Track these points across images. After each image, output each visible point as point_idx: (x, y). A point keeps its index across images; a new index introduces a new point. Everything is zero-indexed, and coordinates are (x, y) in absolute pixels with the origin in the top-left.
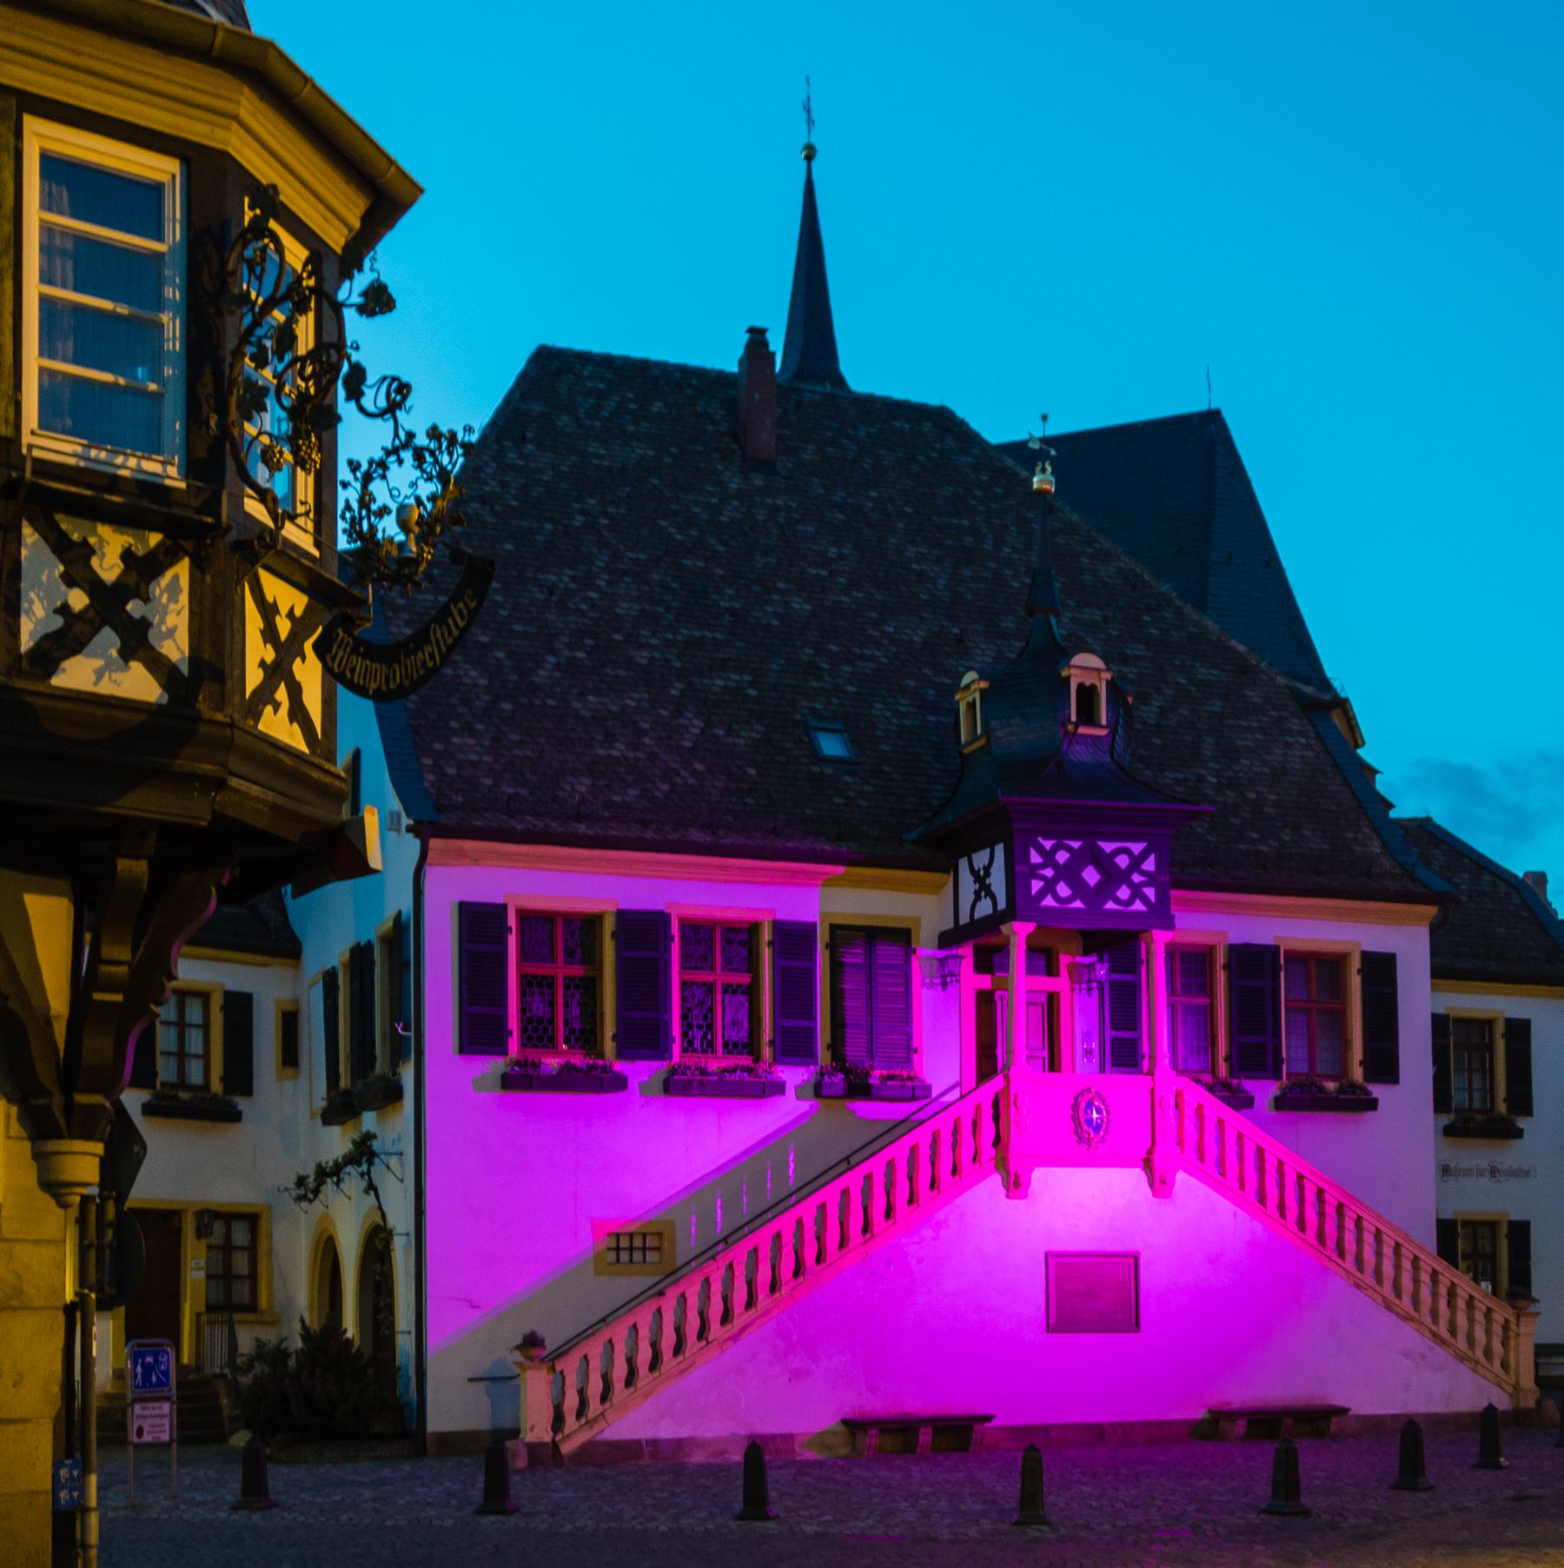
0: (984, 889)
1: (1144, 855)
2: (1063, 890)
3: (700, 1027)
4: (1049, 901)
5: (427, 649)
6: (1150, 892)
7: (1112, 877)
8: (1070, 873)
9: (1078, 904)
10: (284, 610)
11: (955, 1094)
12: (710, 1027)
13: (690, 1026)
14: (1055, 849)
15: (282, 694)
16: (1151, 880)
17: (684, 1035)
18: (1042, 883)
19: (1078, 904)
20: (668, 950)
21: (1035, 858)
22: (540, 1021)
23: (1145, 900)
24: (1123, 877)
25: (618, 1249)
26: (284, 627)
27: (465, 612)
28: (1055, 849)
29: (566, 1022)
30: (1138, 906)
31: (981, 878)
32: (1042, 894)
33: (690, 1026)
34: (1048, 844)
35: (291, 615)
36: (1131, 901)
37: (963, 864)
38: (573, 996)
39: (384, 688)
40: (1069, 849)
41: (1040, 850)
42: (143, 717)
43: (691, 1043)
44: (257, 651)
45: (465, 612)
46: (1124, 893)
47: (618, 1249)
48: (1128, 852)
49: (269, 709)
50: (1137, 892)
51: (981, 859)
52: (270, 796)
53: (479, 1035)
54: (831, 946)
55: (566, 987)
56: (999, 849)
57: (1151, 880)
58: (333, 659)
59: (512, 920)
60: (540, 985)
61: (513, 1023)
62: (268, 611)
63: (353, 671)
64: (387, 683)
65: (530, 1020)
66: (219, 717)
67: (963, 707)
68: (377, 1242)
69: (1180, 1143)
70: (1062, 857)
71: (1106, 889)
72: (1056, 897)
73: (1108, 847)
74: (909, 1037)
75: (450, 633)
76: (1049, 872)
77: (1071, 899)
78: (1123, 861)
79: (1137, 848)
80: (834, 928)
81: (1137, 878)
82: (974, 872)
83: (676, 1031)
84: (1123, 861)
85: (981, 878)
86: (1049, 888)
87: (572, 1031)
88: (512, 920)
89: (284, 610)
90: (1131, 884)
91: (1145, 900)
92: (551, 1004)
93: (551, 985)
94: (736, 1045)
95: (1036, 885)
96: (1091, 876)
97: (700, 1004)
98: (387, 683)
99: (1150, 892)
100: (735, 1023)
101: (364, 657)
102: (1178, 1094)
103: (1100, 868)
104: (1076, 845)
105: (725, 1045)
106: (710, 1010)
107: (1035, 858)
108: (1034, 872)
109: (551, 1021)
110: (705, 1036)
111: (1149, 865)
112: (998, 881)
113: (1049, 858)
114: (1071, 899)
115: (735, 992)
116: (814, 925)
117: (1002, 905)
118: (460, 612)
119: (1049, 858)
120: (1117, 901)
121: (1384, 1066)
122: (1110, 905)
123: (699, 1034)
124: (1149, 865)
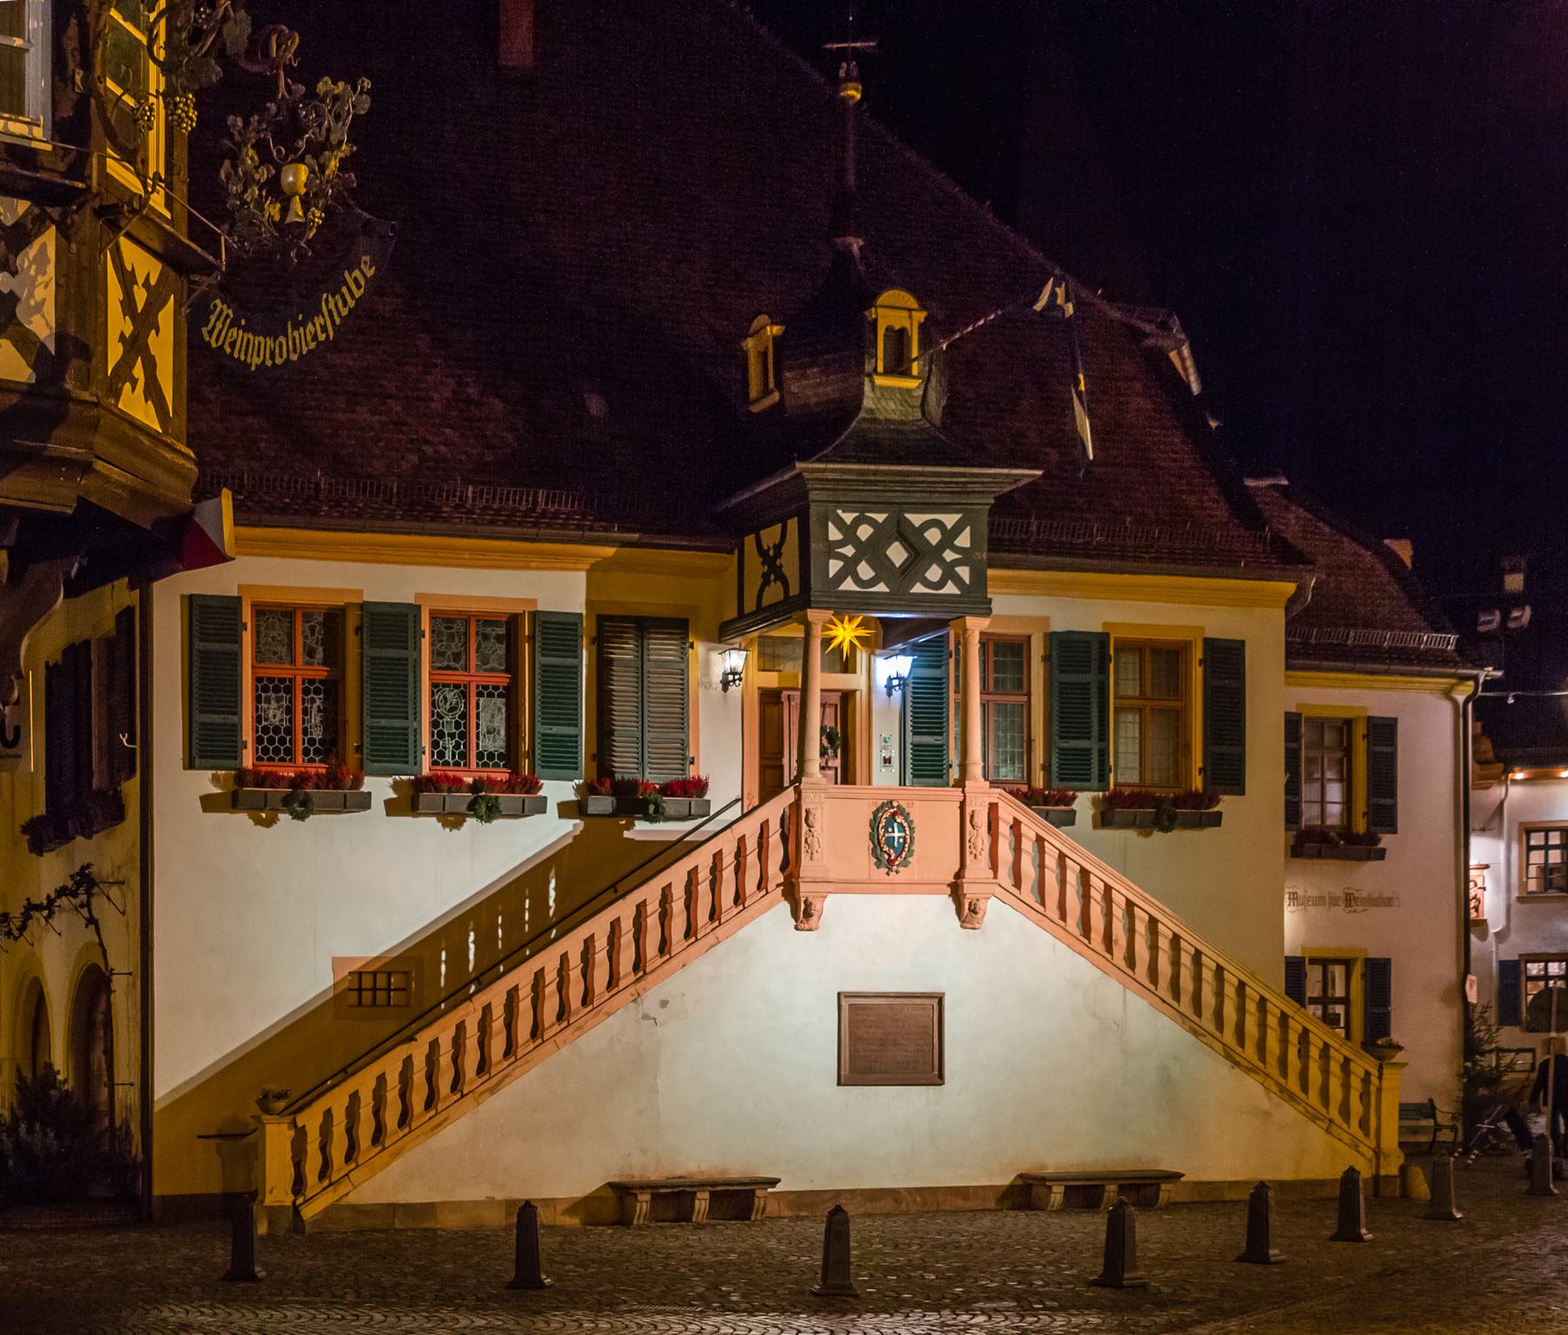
0: (773, 571)
1: (958, 529)
2: (865, 571)
3: (452, 736)
4: (848, 585)
5: (319, 321)
6: (964, 572)
7: (921, 554)
8: (873, 551)
9: (882, 588)
10: (141, 279)
11: (735, 812)
12: (463, 736)
13: (441, 735)
14: (857, 523)
15: (138, 371)
17: (435, 745)
18: (841, 564)
19: (882, 588)
20: (417, 648)
21: (834, 534)
22: (277, 730)
23: (958, 581)
24: (935, 554)
25: (360, 990)
26: (141, 296)
27: (362, 282)
28: (857, 523)
29: (305, 732)
30: (950, 589)
31: (770, 559)
32: (841, 577)
33: (441, 735)
34: (848, 518)
35: (146, 284)
36: (941, 584)
37: (750, 541)
38: (313, 701)
39: (269, 363)
40: (872, 522)
42: (15, 399)
43: (441, 755)
44: (118, 324)
45: (362, 282)
46: (934, 573)
47: (360, 990)
48: (939, 524)
49: (128, 385)
50: (949, 573)
51: (770, 536)
52: (128, 479)
55: (306, 691)
56: (793, 524)
57: (966, 556)
58: (210, 333)
59: (247, 616)
60: (276, 690)
61: (248, 735)
62: (127, 279)
63: (233, 345)
64: (272, 356)
65: (265, 730)
66: (86, 396)
67: (753, 360)
68: (93, 985)
69: (994, 866)
70: (864, 532)
71: (912, 570)
72: (858, 581)
73: (917, 519)
74: (684, 745)
75: (345, 303)
76: (849, 551)
78: (933, 536)
82: (762, 552)
83: (426, 742)
84: (933, 536)
85: (770, 559)
86: (849, 568)
87: (312, 742)
89: (141, 279)
92: (289, 711)
93: (289, 690)
94: (491, 756)
95: (835, 566)
96: (897, 554)
97: (452, 709)
98: (272, 356)
101: (246, 329)
102: (993, 807)
104: (880, 518)
105: (480, 756)
106: (463, 716)
107: (834, 534)
108: (831, 550)
109: (289, 731)
110: (457, 746)
112: (789, 562)
113: (849, 532)
115: (491, 695)
117: (794, 589)
118: (356, 280)
119: (849, 532)
120: (928, 584)
121: (1228, 772)
123: (450, 744)
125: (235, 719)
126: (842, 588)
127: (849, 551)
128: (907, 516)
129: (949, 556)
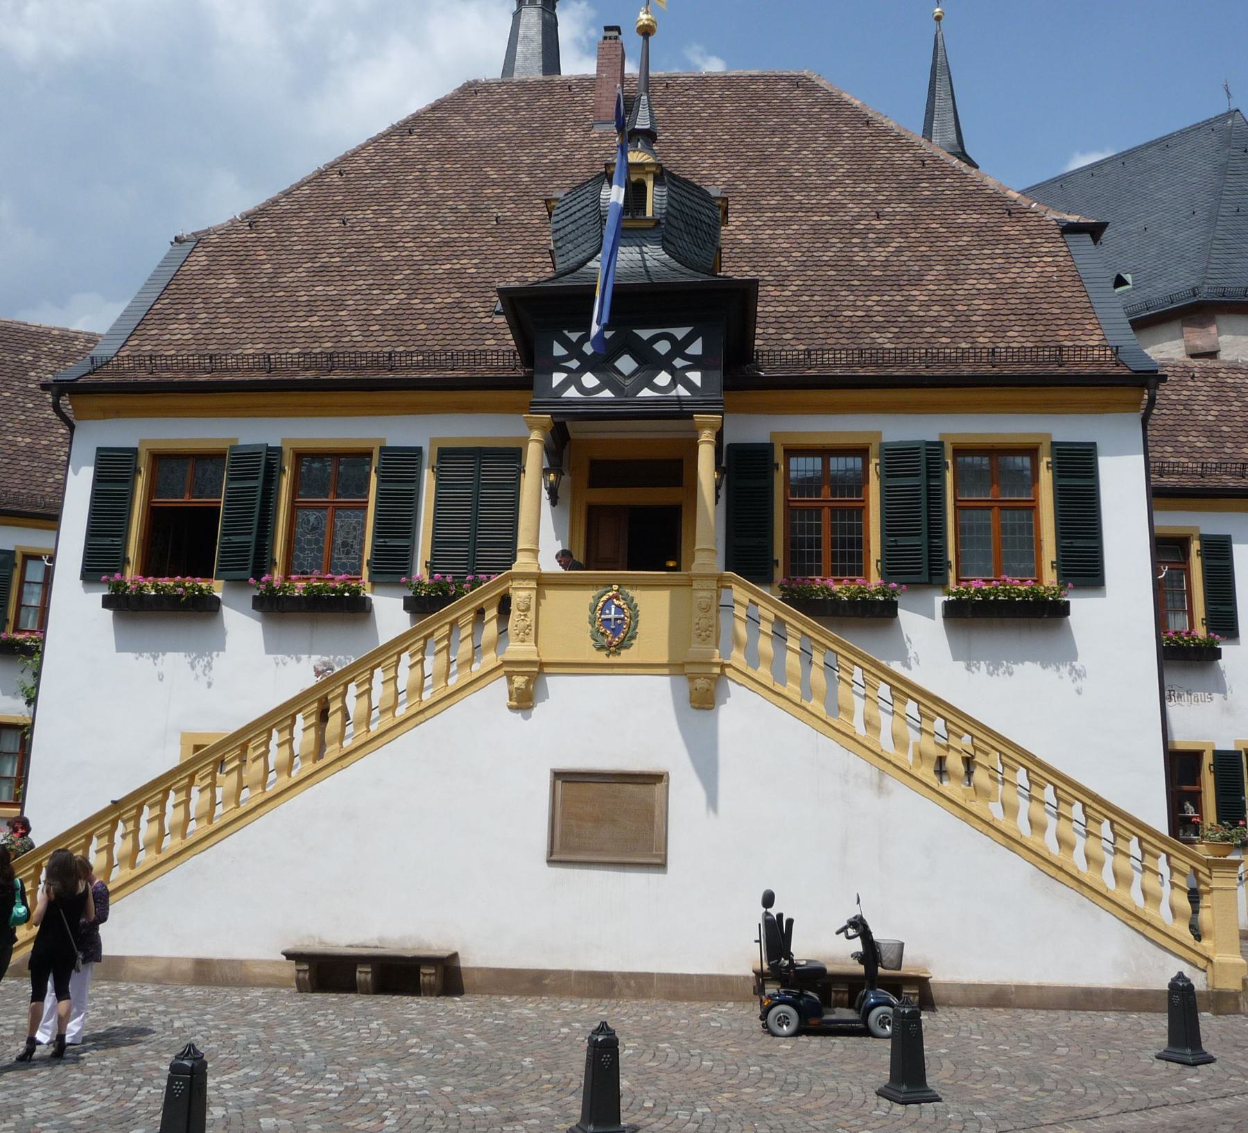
1: (689, 340)
2: (589, 380)
3: (312, 550)
4: (572, 393)
16: (696, 363)
18: (564, 375)
21: (559, 350)
23: (689, 385)
24: (664, 363)
30: (682, 391)
32: (564, 385)
41: (566, 343)
46: (663, 379)
53: (97, 565)
59: (143, 464)
72: (581, 388)
73: (645, 334)
76: (574, 364)
77: (597, 389)
78: (663, 347)
79: (680, 333)
84: (663, 347)
88: (143, 464)
90: (672, 370)
96: (626, 364)
100: (345, 544)
107: (559, 350)
111: (696, 348)
114: (597, 389)
119: (574, 350)
120: (654, 388)
122: (646, 393)
124: (696, 348)
125: (118, 541)
126: (565, 395)
129: (679, 363)
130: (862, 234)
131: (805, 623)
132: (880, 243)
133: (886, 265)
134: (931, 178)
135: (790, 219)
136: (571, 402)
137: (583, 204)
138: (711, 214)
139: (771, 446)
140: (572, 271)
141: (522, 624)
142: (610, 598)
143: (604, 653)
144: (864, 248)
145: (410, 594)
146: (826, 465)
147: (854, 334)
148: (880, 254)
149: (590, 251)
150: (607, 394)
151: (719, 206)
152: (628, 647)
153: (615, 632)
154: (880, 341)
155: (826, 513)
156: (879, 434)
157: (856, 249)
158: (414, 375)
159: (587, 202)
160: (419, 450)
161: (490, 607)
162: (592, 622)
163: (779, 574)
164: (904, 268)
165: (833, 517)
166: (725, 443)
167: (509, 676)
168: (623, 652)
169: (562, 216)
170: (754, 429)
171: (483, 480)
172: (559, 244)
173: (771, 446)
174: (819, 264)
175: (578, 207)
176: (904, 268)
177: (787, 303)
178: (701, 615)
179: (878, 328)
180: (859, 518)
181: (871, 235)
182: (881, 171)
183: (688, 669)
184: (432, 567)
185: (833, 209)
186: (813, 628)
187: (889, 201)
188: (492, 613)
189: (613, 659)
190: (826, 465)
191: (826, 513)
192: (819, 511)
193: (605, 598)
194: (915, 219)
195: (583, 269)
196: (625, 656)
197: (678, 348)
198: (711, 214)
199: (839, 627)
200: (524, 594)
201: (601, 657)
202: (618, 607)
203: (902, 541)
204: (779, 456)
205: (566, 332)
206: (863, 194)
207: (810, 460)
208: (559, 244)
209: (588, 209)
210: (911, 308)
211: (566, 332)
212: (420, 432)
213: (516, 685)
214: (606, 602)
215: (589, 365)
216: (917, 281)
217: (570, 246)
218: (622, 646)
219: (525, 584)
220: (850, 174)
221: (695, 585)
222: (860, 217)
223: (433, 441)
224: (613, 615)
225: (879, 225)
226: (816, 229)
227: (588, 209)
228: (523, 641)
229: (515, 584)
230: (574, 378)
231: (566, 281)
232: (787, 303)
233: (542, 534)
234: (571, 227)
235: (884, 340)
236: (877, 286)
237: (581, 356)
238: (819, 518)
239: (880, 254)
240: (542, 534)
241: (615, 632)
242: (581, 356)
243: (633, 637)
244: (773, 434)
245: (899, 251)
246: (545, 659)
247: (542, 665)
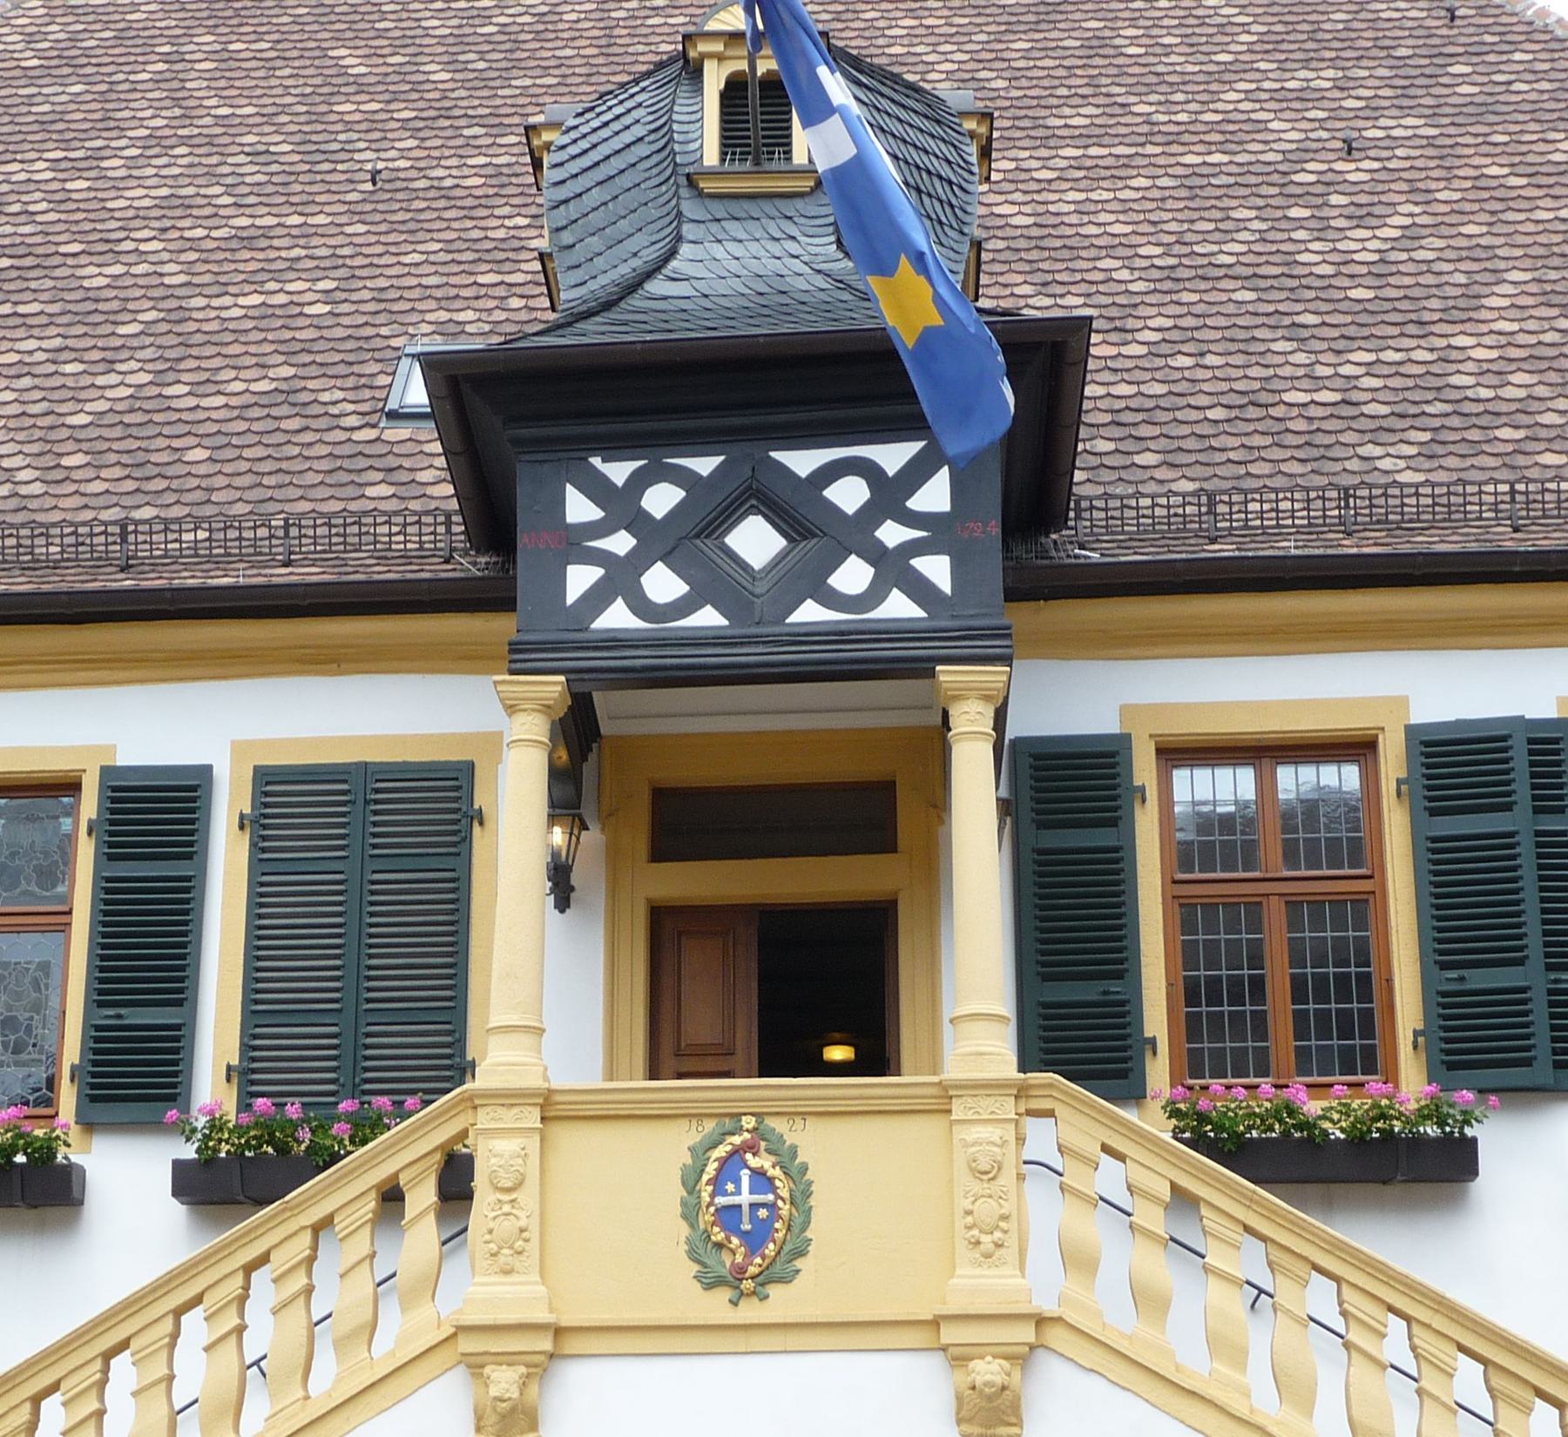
2: (662, 584)
4: (617, 617)
6: (937, 569)
14: (639, 483)
18: (599, 572)
21: (579, 508)
23: (920, 589)
24: (854, 534)
28: (639, 483)
30: (898, 606)
32: (597, 598)
34: (619, 472)
36: (874, 595)
41: (598, 489)
46: (853, 576)
54: (257, 824)
70: (661, 500)
72: (641, 605)
73: (802, 462)
77: (684, 607)
78: (849, 495)
80: (266, 779)
81: (892, 534)
84: (849, 495)
86: (621, 579)
90: (877, 555)
91: (920, 589)
96: (756, 541)
99: (937, 569)
103: (728, 516)
104: (705, 466)
107: (579, 508)
111: (935, 496)
114: (684, 607)
116: (205, 772)
119: (621, 507)
122: (810, 613)
124: (935, 496)
127: (621, 543)
128: (773, 454)
129: (892, 534)
130: (1317, 196)
131: (1250, 1202)
132: (1363, 217)
133: (1381, 271)
134: (1474, 53)
135: (1126, 163)
136: (616, 641)
137: (627, 137)
138: (952, 155)
139: (1124, 740)
140: (608, 305)
141: (507, 1227)
142: (737, 1152)
143: (724, 1294)
144: (1322, 229)
145: (189, 1152)
146: (1266, 786)
147: (1316, 449)
148: (1364, 245)
149: (651, 254)
150: (708, 618)
151: (972, 135)
152: (785, 1279)
153: (754, 1241)
154: (1386, 464)
155: (1275, 914)
156: (1402, 702)
157: (1300, 235)
158: (190, 580)
159: (639, 131)
160: (205, 772)
161: (417, 1181)
162: (690, 1213)
163: (1158, 1073)
164: (1429, 279)
165: (1294, 924)
166: (1010, 735)
167: (475, 1366)
168: (774, 1291)
169: (574, 167)
170: (1077, 697)
171: (379, 850)
172: (567, 237)
173: (1124, 740)
174: (1209, 275)
175: (616, 144)
176: (1429, 279)
177: (1138, 375)
178: (977, 1187)
179: (1379, 432)
180: (1361, 923)
181: (1335, 199)
182: (1347, 37)
183: (949, 1334)
184: (245, 1077)
185: (1232, 134)
186: (1271, 1215)
187: (1372, 112)
188: (422, 1197)
189: (750, 1312)
190: (1266, 786)
191: (1275, 914)
192: (1255, 908)
193: (721, 1151)
194: (1445, 156)
195: (635, 301)
196: (781, 1303)
197: (890, 496)
198: (952, 155)
199: (1327, 1206)
200: (506, 1146)
201: (716, 1306)
202: (758, 1173)
203: (1479, 979)
204: (1144, 769)
205: (596, 461)
206: (1304, 96)
207: (1224, 774)
208: (567, 237)
209: (642, 150)
210: (1456, 380)
211: (596, 461)
212: (218, 726)
213: (494, 1391)
214: (724, 1162)
215: (660, 540)
216: (1465, 309)
217: (595, 243)
218: (766, 1279)
219: (508, 1117)
220: (1269, 45)
221: (959, 1110)
222: (1307, 151)
223: (239, 749)
224: (745, 1198)
225: (1355, 172)
226: (1194, 184)
227: (642, 150)
228: (507, 1272)
229: (484, 1119)
230: (621, 579)
231: (594, 332)
232: (1138, 375)
233: (542, 977)
234: (596, 196)
235: (1396, 462)
236: (1362, 327)
237: (638, 522)
238: (1255, 925)
239: (1364, 245)
240: (542, 977)
241: (754, 1241)
242: (638, 522)
243: (801, 1253)
244: (1126, 711)
245: (1411, 235)
246: (566, 1321)
247: (559, 1332)
